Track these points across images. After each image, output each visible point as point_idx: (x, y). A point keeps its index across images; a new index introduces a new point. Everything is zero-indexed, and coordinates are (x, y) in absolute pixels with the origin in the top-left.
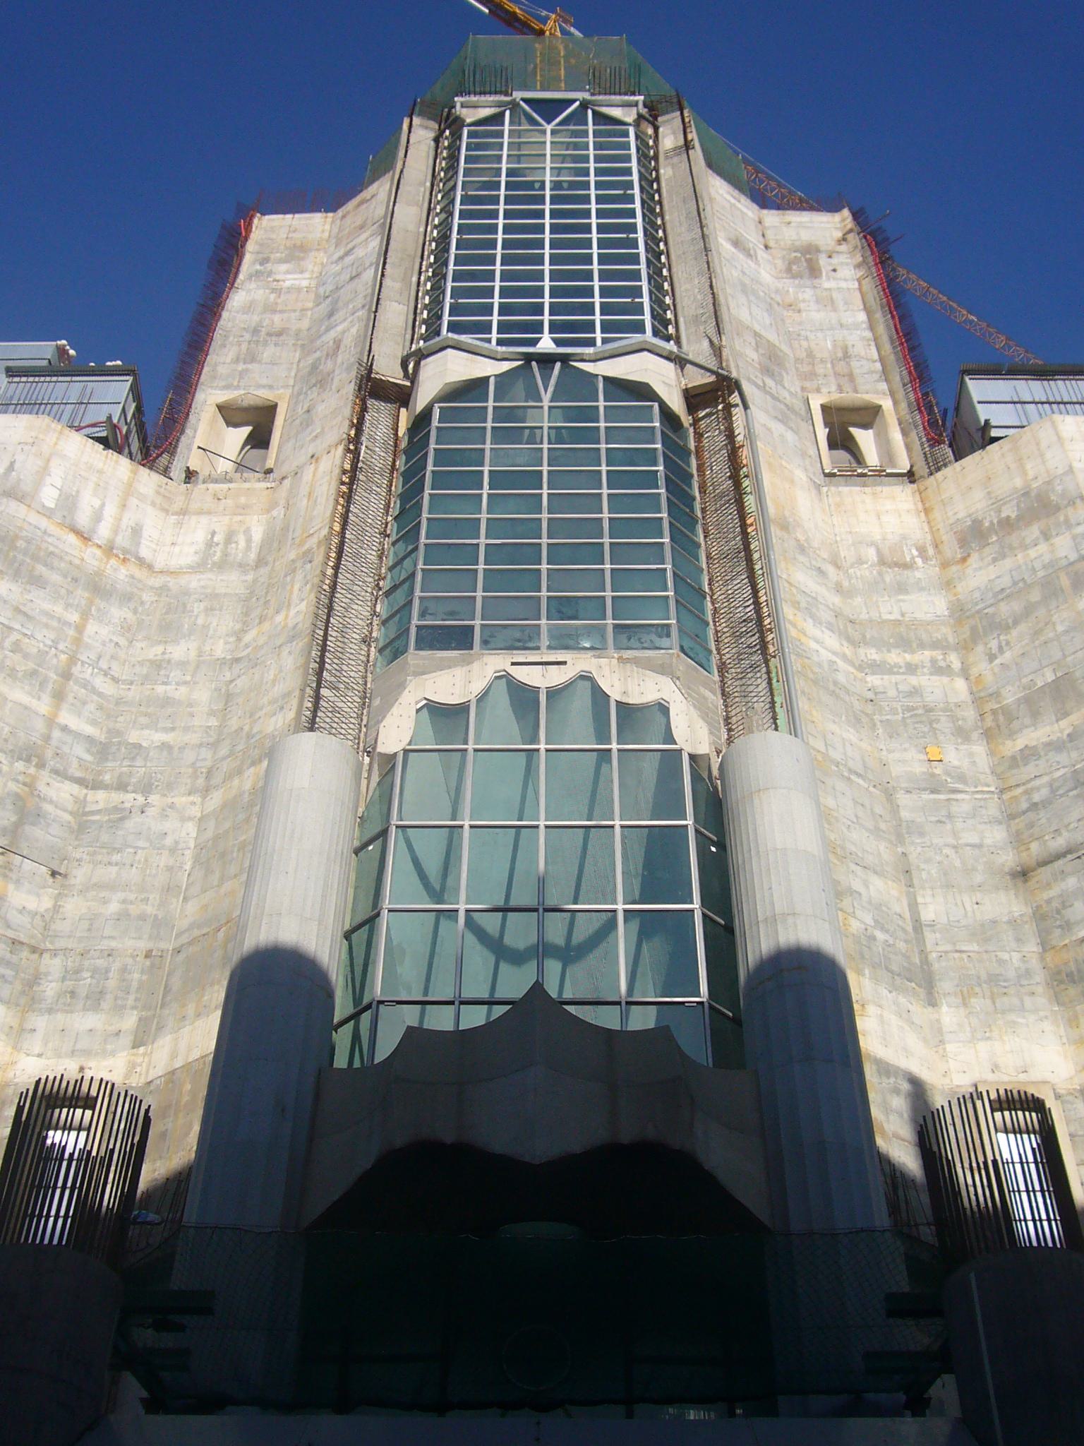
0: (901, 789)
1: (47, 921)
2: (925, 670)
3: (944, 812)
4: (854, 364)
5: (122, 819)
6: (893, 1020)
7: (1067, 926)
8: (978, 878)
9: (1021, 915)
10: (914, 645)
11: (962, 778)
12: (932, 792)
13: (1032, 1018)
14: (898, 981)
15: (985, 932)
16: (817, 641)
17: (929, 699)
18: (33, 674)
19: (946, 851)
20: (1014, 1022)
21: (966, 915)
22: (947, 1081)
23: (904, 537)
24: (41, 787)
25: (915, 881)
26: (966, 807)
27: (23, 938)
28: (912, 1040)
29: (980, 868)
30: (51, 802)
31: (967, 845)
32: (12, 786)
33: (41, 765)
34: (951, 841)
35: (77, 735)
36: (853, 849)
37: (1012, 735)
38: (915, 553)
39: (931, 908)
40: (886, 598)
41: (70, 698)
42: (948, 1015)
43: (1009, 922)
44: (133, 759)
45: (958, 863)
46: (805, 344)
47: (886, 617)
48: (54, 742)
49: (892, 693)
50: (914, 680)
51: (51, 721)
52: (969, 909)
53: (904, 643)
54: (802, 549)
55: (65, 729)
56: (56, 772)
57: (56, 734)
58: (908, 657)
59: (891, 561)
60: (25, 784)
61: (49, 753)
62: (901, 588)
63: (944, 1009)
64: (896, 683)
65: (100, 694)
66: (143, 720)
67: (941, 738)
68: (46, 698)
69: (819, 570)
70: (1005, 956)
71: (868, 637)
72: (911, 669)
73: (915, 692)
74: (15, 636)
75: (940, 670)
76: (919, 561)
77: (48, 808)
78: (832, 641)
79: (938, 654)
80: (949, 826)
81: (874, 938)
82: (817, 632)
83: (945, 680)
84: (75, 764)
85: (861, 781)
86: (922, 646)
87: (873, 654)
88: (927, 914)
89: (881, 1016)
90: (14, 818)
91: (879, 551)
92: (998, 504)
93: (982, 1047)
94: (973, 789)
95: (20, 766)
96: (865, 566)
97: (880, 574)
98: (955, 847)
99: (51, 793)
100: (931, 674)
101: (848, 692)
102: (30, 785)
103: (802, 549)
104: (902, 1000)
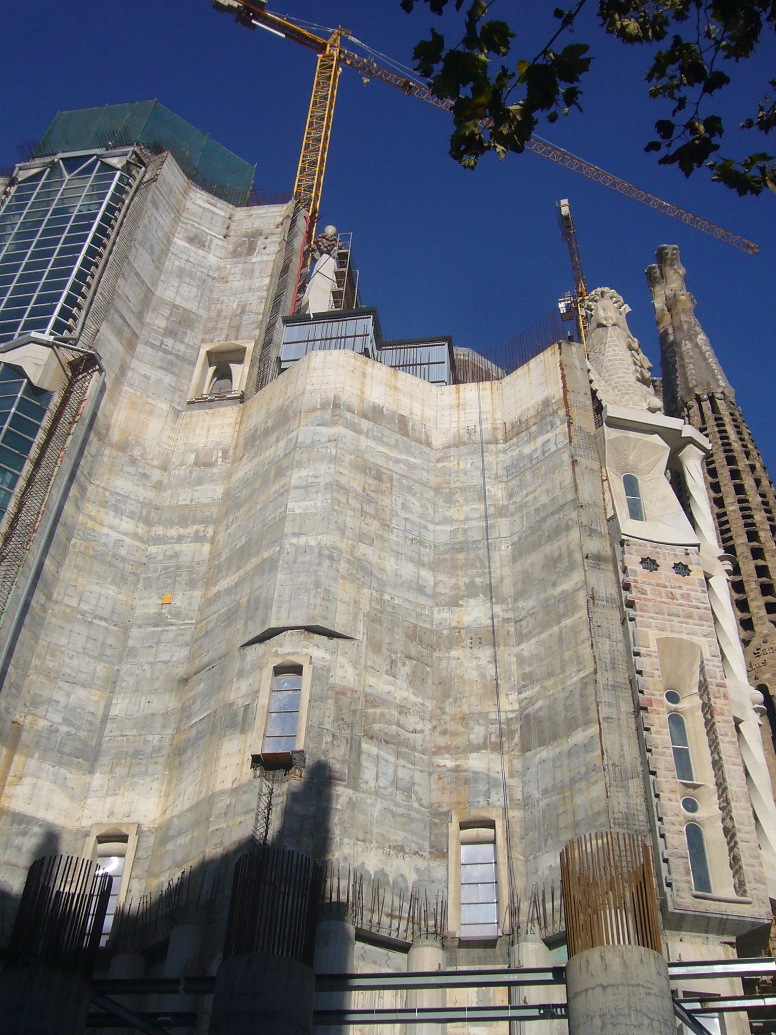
0: (136, 625)
2: (189, 540)
3: (155, 640)
4: (245, 317)
7: (188, 718)
8: (157, 684)
9: (173, 709)
10: (189, 522)
11: (177, 615)
12: (154, 626)
13: (148, 779)
15: (145, 723)
16: (111, 527)
17: (183, 560)
19: (146, 667)
21: (138, 711)
23: (218, 444)
25: (117, 690)
26: (171, 635)
28: (60, 799)
29: (162, 677)
31: (160, 662)
34: (152, 660)
36: (69, 671)
37: (215, 585)
38: (220, 454)
39: (119, 706)
40: (187, 489)
43: (163, 714)
45: (148, 675)
46: (219, 306)
47: (180, 503)
49: (160, 557)
50: (177, 547)
52: (142, 706)
53: (184, 522)
54: (133, 461)
58: (181, 530)
59: (202, 462)
62: (200, 481)
63: (97, 775)
64: (166, 550)
67: (177, 587)
69: (145, 476)
70: (150, 738)
71: (163, 518)
72: (180, 539)
73: (176, 555)
75: (198, 538)
76: (220, 460)
78: (127, 525)
79: (200, 527)
80: (154, 650)
81: (57, 731)
82: (116, 522)
83: (198, 545)
85: (103, 623)
86: (194, 523)
87: (160, 531)
88: (114, 712)
91: (197, 457)
92: (268, 416)
93: (109, 800)
94: (181, 622)
96: (184, 467)
97: (191, 472)
98: (152, 664)
100: (191, 542)
101: (124, 560)
103: (133, 461)
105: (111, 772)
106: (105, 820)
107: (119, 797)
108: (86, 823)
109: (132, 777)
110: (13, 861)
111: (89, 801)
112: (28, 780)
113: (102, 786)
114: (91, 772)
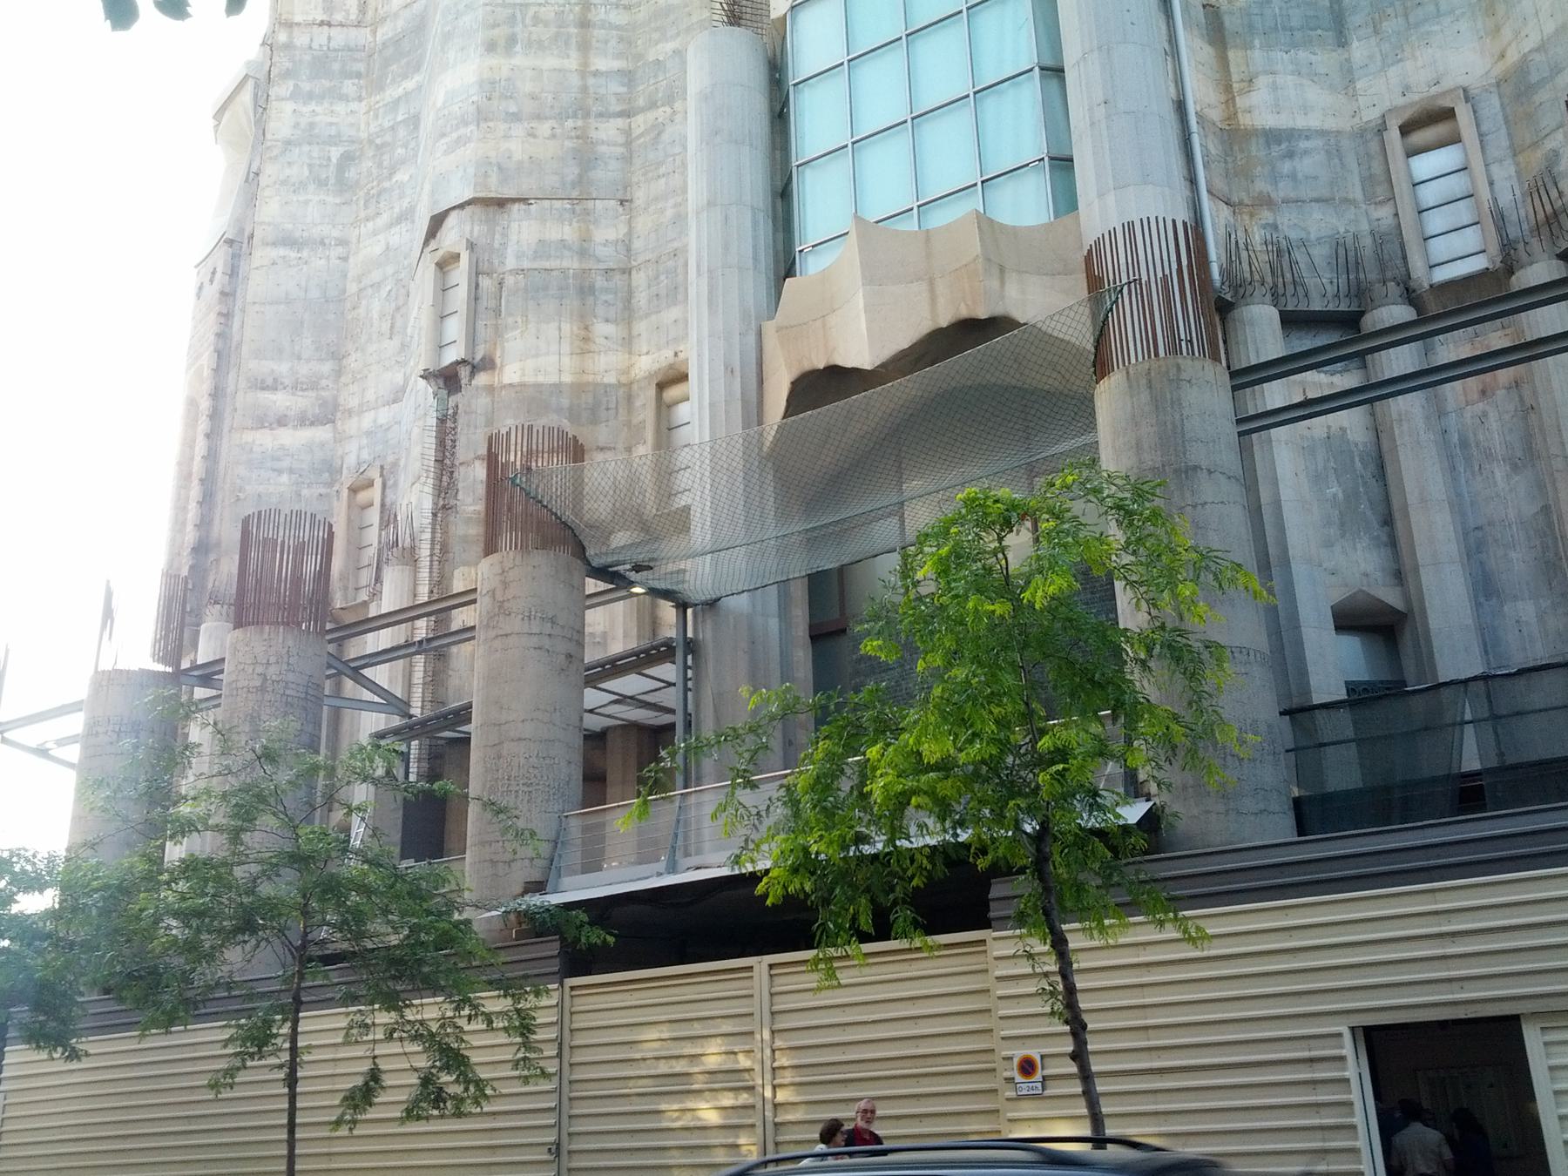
1: (627, 245)
5: (659, 134)
6: (1289, 80)
14: (1298, 35)
18: (557, 36)
20: (1428, 33)
22: (1356, 120)
24: (593, 134)
27: (612, 265)
28: (1315, 95)
30: (603, 142)
32: (569, 144)
33: (587, 115)
35: (607, 74)
41: (594, 43)
42: (1359, 50)
44: (655, 76)
48: (591, 90)
51: (584, 72)
55: (596, 74)
56: (601, 115)
57: (591, 81)
60: (578, 137)
61: (590, 101)
63: (1355, 44)
65: (618, 28)
66: (656, 36)
68: (574, 54)
74: (531, 13)
77: (603, 149)
84: (613, 100)
89: (1274, 83)
90: (576, 172)
93: (1393, 72)
95: (570, 123)
99: (602, 135)
102: (582, 136)
104: (1303, 55)
105: (1376, 32)
106: (1401, 101)
107: (1409, 64)
108: (1371, 115)
109: (1417, 25)
110: (1292, 195)
111: (1359, 85)
112: (1262, 81)
113: (1371, 57)
114: (1342, 42)
